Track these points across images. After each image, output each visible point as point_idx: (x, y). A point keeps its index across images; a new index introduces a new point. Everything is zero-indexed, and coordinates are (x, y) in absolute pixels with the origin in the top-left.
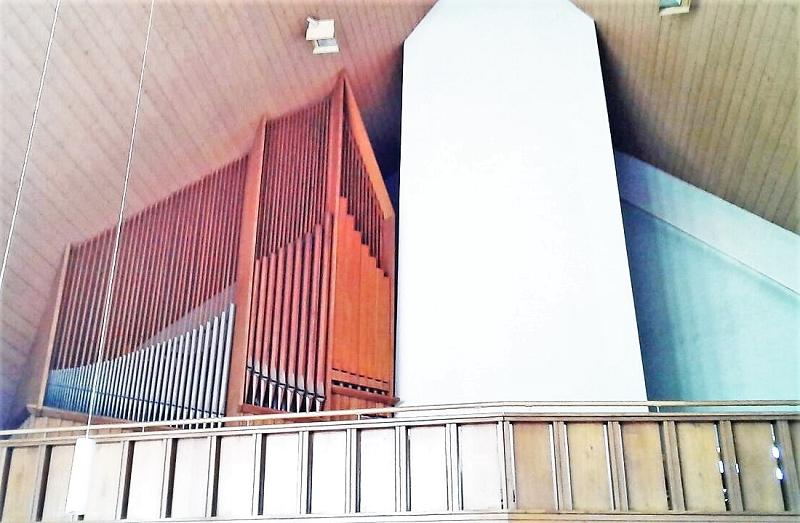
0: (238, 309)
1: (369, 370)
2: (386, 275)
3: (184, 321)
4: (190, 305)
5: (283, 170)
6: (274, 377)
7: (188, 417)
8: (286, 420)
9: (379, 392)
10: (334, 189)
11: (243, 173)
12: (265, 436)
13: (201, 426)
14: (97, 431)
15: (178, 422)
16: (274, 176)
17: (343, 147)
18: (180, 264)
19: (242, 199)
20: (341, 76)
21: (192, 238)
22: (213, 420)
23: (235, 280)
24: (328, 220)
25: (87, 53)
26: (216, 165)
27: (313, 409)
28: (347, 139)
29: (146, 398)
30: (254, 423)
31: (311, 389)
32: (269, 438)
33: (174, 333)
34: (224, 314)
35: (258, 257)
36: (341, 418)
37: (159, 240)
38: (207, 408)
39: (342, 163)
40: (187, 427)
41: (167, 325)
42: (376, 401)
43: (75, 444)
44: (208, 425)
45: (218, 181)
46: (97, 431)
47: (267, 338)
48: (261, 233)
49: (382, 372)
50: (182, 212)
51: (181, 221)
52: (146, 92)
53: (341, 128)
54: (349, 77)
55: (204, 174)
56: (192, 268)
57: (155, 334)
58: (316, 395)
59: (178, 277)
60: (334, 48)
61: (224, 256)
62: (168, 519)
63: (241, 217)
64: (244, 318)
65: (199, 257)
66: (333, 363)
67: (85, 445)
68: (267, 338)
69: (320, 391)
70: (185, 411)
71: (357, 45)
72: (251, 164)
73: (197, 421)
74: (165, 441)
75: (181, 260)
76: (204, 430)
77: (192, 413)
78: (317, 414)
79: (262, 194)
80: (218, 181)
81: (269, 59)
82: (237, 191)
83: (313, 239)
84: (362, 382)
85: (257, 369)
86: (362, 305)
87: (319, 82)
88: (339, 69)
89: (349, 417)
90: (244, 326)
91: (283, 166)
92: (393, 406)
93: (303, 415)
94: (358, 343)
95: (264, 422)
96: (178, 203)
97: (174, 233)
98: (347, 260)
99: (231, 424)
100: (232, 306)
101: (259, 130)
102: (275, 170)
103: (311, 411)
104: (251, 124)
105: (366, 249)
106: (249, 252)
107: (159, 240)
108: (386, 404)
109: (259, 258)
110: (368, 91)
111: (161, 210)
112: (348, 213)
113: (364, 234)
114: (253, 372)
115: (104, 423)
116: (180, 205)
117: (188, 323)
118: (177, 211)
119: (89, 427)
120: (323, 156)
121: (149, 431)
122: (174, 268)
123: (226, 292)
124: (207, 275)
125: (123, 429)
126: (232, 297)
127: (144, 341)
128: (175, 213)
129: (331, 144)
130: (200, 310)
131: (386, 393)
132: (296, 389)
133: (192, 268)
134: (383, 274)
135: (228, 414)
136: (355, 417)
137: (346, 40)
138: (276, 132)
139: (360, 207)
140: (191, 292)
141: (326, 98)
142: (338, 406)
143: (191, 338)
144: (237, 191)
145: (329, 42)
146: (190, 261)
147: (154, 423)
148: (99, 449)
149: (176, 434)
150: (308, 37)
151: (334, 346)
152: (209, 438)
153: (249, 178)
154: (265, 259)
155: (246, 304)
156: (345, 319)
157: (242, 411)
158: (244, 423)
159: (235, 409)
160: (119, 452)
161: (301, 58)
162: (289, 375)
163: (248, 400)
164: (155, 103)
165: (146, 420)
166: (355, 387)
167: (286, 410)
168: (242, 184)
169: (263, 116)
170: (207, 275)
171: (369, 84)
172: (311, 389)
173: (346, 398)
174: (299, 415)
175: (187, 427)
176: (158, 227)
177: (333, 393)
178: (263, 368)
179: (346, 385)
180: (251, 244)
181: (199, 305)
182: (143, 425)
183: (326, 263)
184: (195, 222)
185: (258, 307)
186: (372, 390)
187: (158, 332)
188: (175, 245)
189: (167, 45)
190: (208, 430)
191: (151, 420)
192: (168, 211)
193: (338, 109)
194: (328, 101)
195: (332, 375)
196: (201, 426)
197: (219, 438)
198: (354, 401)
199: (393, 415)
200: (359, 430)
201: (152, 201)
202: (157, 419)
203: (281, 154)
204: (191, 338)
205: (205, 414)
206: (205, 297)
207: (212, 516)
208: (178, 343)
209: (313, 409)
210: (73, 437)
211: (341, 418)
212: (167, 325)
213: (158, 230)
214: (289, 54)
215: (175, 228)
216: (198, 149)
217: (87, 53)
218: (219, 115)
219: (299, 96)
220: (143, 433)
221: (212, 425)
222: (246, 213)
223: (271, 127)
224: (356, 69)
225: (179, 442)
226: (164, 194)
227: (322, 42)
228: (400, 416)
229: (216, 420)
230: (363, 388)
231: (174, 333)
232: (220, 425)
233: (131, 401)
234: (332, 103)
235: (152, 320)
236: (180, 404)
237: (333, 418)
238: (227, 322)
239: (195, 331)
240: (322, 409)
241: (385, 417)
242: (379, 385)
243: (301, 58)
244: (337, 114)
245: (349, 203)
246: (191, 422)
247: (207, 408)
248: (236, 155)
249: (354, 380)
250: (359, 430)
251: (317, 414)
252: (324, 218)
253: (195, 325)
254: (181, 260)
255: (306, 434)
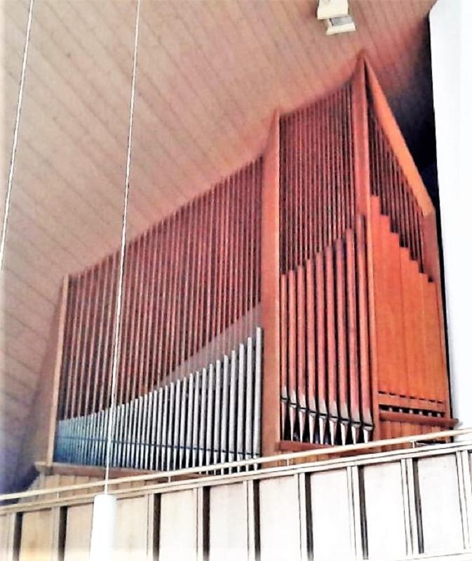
0: (265, 332)
1: (423, 392)
2: (430, 280)
3: (205, 353)
4: (211, 333)
5: (303, 171)
6: (313, 407)
7: (219, 461)
8: (331, 456)
9: (434, 414)
10: (363, 186)
11: (259, 178)
12: (308, 475)
13: (235, 470)
14: (117, 486)
15: (208, 468)
16: (294, 179)
17: (370, 139)
18: (195, 287)
19: (259, 207)
20: (360, 57)
21: (207, 256)
22: (248, 462)
23: (259, 300)
24: (359, 223)
25: (69, 56)
26: (228, 169)
27: (361, 440)
28: (374, 128)
29: (169, 442)
30: (294, 462)
31: (356, 417)
32: (313, 478)
33: (195, 366)
34: (250, 340)
35: (283, 271)
36: (394, 447)
37: (169, 263)
38: (239, 449)
39: (370, 156)
40: (218, 472)
41: (186, 358)
42: (431, 425)
43: (93, 503)
44: (243, 469)
45: (231, 189)
46: (117, 486)
47: (301, 365)
48: (284, 244)
49: (437, 392)
50: (193, 227)
51: (192, 238)
52: (140, 94)
53: (365, 117)
54: (369, 57)
55: (215, 183)
56: (209, 291)
57: (173, 369)
58: (362, 424)
59: (195, 302)
60: (350, 26)
61: (244, 274)
62: (422, 555)
63: (260, 228)
64: (274, 342)
65: (216, 277)
66: (379, 385)
67: (104, 503)
68: (301, 365)
69: (367, 419)
70: (215, 454)
71: (376, 21)
72: (267, 166)
73: (231, 465)
74: (195, 490)
75: (195, 283)
76: (239, 474)
77: (223, 455)
78: (367, 445)
79: (283, 199)
80: (231, 189)
81: (277, 45)
82: (253, 198)
83: (345, 246)
84: (414, 404)
85: (293, 400)
86: (406, 316)
87: (337, 66)
88: (358, 49)
89: (402, 446)
90: (274, 352)
91: (303, 166)
92: (451, 429)
93: (350, 447)
94: (406, 361)
95: (305, 460)
96: (188, 218)
97: (185, 253)
98: (385, 267)
99: (269, 465)
100: (259, 330)
101: (272, 128)
102: (294, 171)
103: (347, 443)
104: (262, 121)
105: (405, 252)
106: (273, 267)
107: (169, 263)
108: (443, 427)
109: (284, 273)
110: (392, 72)
111: (168, 227)
112: (382, 213)
113: (401, 236)
114: (288, 403)
115: (124, 475)
116: (190, 221)
117: (209, 355)
118: (187, 228)
119: (107, 482)
120: (348, 151)
121: (175, 480)
122: (189, 293)
123: (250, 315)
124: (228, 297)
125: (146, 481)
126: (257, 319)
127: (161, 379)
128: (184, 230)
129: (355, 136)
130: (220, 340)
131: (443, 414)
132: (340, 419)
133: (209, 291)
134: (427, 279)
135: (265, 452)
136: (410, 445)
137: (363, 15)
138: (292, 128)
139: (395, 205)
140: (211, 318)
141: (346, 84)
142: (389, 434)
143: (215, 370)
144: (253, 198)
145: (343, 20)
146: (206, 282)
147: (181, 472)
148: (120, 506)
149: (208, 481)
150: (322, 13)
151: (378, 365)
152: (245, 483)
153: (266, 182)
154: (291, 273)
155: (274, 327)
156: (388, 333)
157: (281, 449)
158: (282, 463)
159: (272, 447)
160: (143, 508)
161: (313, 41)
162: (330, 403)
163: (286, 436)
164: (151, 106)
165: (171, 469)
166: (406, 410)
167: (330, 443)
168: (258, 190)
169: (275, 111)
170: (228, 297)
171: (393, 64)
172: (356, 417)
173: (397, 425)
174: (345, 448)
175: (218, 472)
176: (167, 246)
177: (382, 419)
178: (300, 397)
179: (396, 409)
180: (274, 258)
181: (221, 331)
182: (169, 474)
183: (361, 272)
184: (208, 238)
185: (288, 329)
186: (425, 412)
187: (177, 368)
188: (188, 266)
189: (159, 39)
190: (243, 473)
191: (177, 468)
192: (176, 228)
193: (360, 95)
194: (348, 87)
195: (379, 400)
196: (235, 470)
197: (257, 482)
198: (407, 427)
199: (452, 439)
200: (415, 460)
201: (157, 218)
202: (190, 465)
203: (300, 152)
204: (215, 370)
205: (238, 455)
206: (227, 322)
207: (420, 552)
208: (201, 377)
209: (361, 440)
210: (90, 495)
211: (394, 447)
212: (186, 358)
213: (167, 250)
214: (299, 37)
215: (186, 247)
216: (205, 155)
217: (69, 56)
218: (226, 114)
219: (315, 87)
220: (170, 484)
221: (247, 468)
222: (265, 222)
223: (286, 123)
224: (377, 47)
225: (212, 491)
226: (170, 208)
227: (336, 21)
228: (461, 439)
229: (251, 462)
230: (416, 411)
231: (195, 366)
232: (256, 466)
233: (152, 448)
234: (353, 89)
235: (169, 353)
236: (208, 446)
237: (384, 449)
238: (254, 348)
239: (211, 366)
240: (371, 439)
241: (443, 442)
242: (434, 407)
243: (313, 41)
244: (360, 101)
245: (382, 201)
246: (223, 466)
247: (239, 449)
248: (250, 157)
249: (405, 403)
250: (415, 460)
251: (367, 445)
252: (355, 221)
253: (218, 355)
254: (195, 283)
255: (355, 470)
